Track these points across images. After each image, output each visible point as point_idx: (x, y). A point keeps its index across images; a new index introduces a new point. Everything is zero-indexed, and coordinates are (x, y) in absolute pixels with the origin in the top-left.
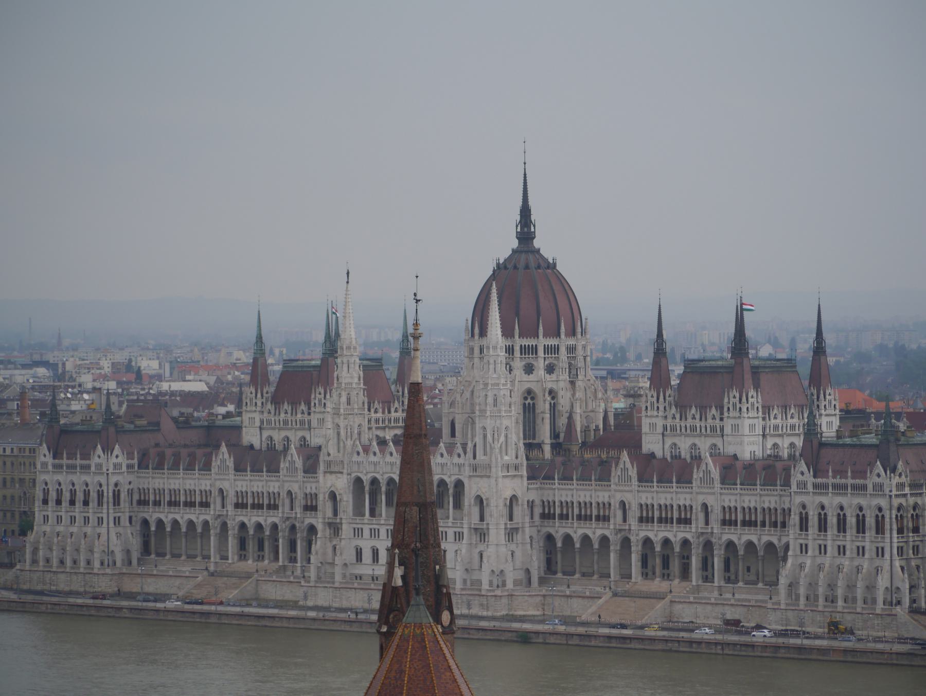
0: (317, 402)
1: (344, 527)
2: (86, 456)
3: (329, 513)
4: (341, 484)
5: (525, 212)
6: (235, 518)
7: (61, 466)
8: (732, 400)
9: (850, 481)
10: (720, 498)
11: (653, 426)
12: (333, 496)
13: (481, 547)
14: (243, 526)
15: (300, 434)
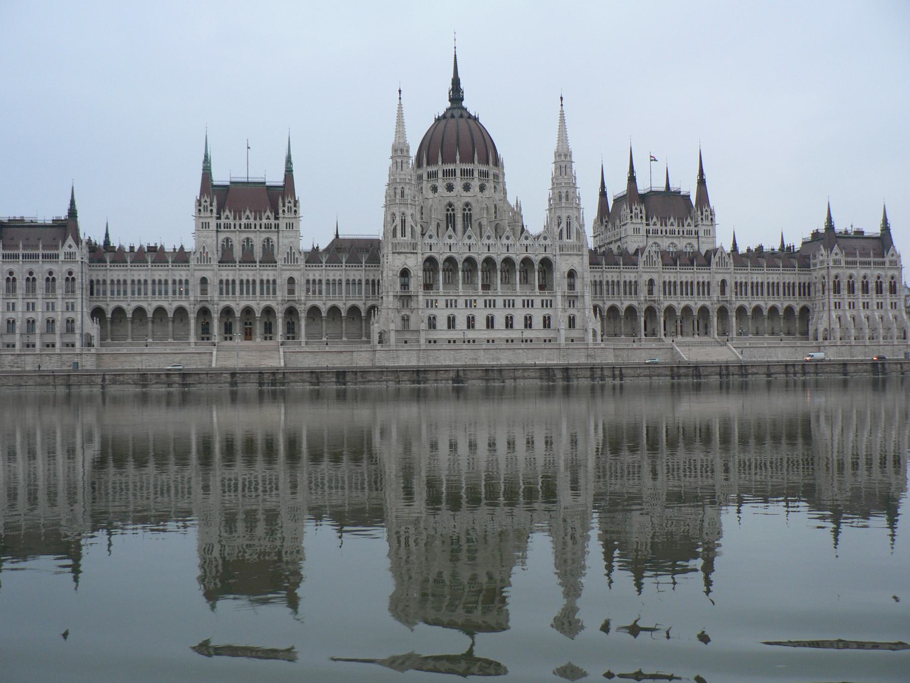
0: (286, 209)
1: (421, 298)
2: (56, 247)
3: (398, 288)
4: (415, 263)
5: (456, 82)
6: (217, 302)
7: (16, 256)
8: (704, 213)
9: (872, 259)
10: (734, 276)
11: (636, 231)
12: (405, 273)
13: (572, 311)
14: (227, 312)
15: (265, 236)
